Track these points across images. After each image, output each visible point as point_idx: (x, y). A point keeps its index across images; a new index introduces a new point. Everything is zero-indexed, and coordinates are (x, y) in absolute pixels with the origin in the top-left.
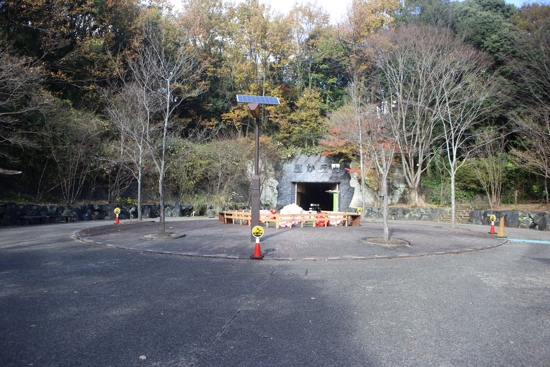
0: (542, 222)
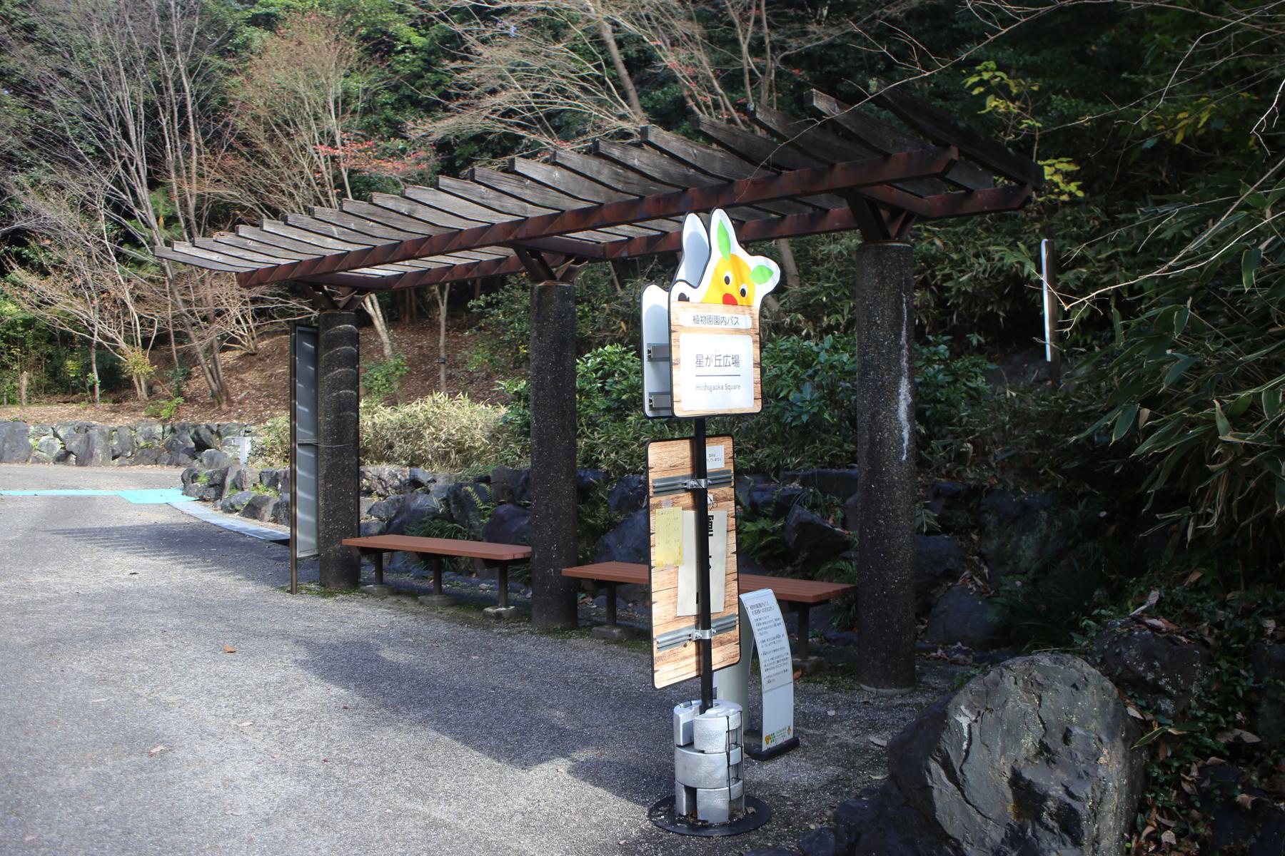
0: (83, 446)
